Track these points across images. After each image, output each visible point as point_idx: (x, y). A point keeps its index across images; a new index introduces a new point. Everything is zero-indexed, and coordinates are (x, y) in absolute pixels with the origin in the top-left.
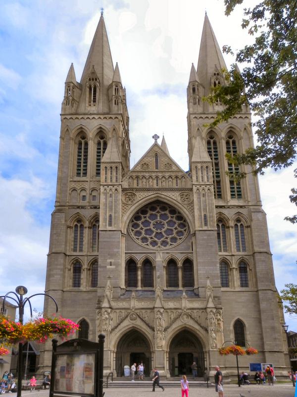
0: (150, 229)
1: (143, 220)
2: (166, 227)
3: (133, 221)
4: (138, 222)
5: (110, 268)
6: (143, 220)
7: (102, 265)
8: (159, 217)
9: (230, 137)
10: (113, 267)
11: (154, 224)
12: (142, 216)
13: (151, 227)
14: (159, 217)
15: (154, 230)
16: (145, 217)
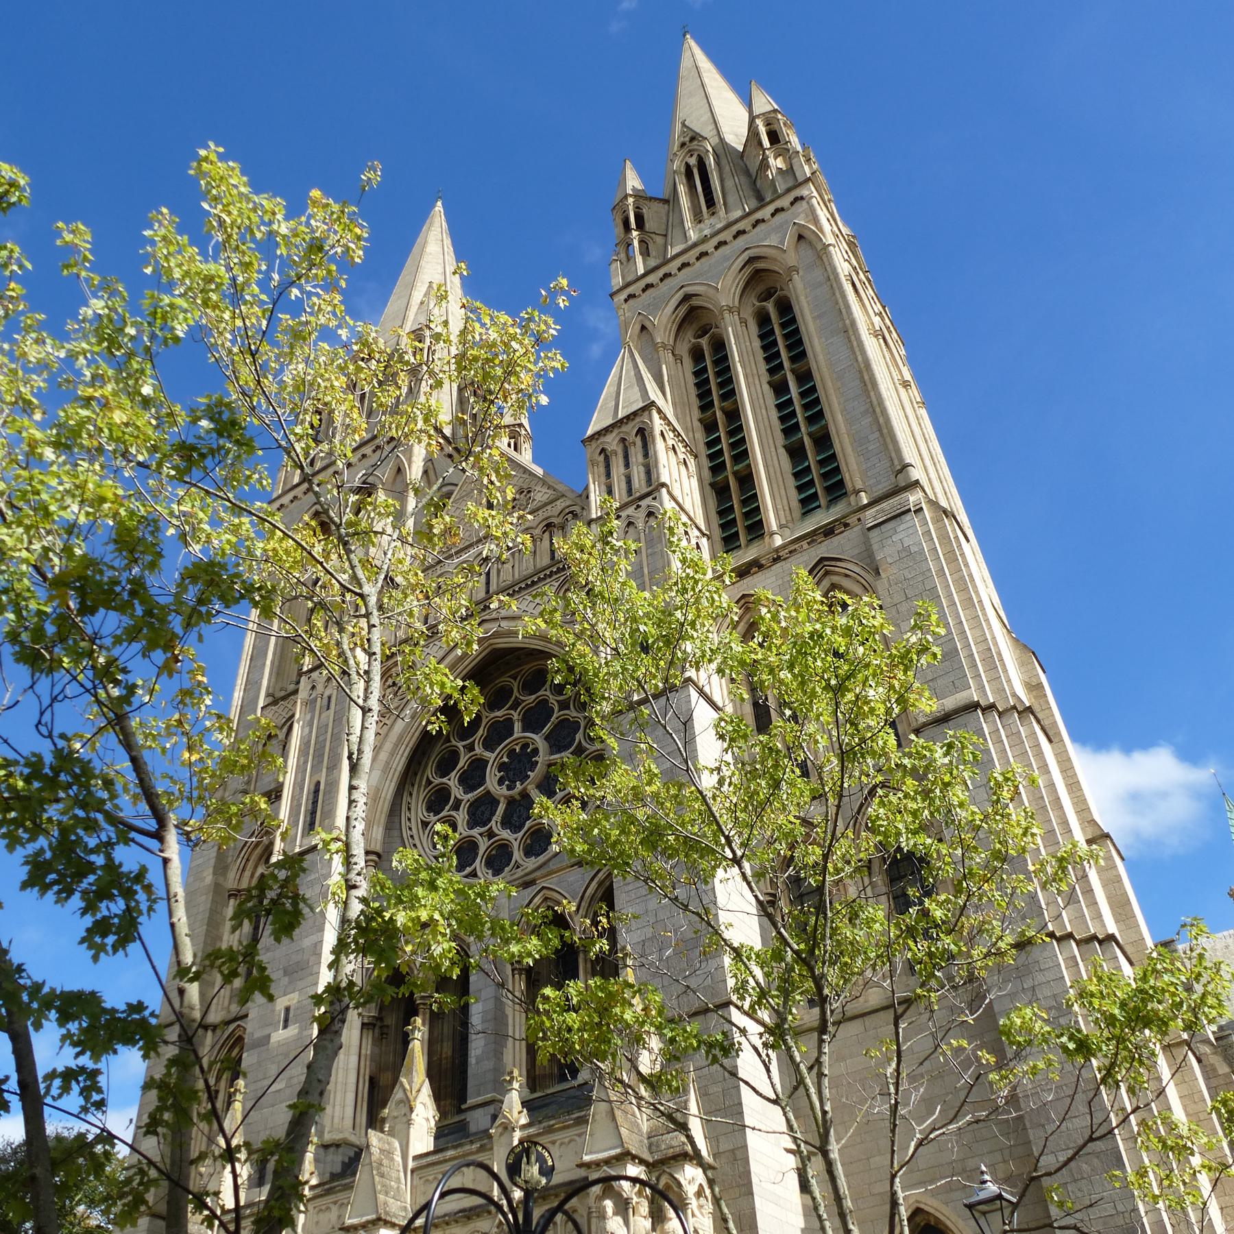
0: (488, 792)
1: (463, 762)
2: (542, 758)
3: (429, 782)
4: (445, 780)
5: (280, 1044)
6: (463, 762)
7: (257, 1035)
8: (517, 726)
9: (767, 295)
10: (293, 1030)
11: (502, 767)
12: (460, 745)
13: (492, 781)
14: (517, 726)
15: (501, 792)
16: (470, 748)
